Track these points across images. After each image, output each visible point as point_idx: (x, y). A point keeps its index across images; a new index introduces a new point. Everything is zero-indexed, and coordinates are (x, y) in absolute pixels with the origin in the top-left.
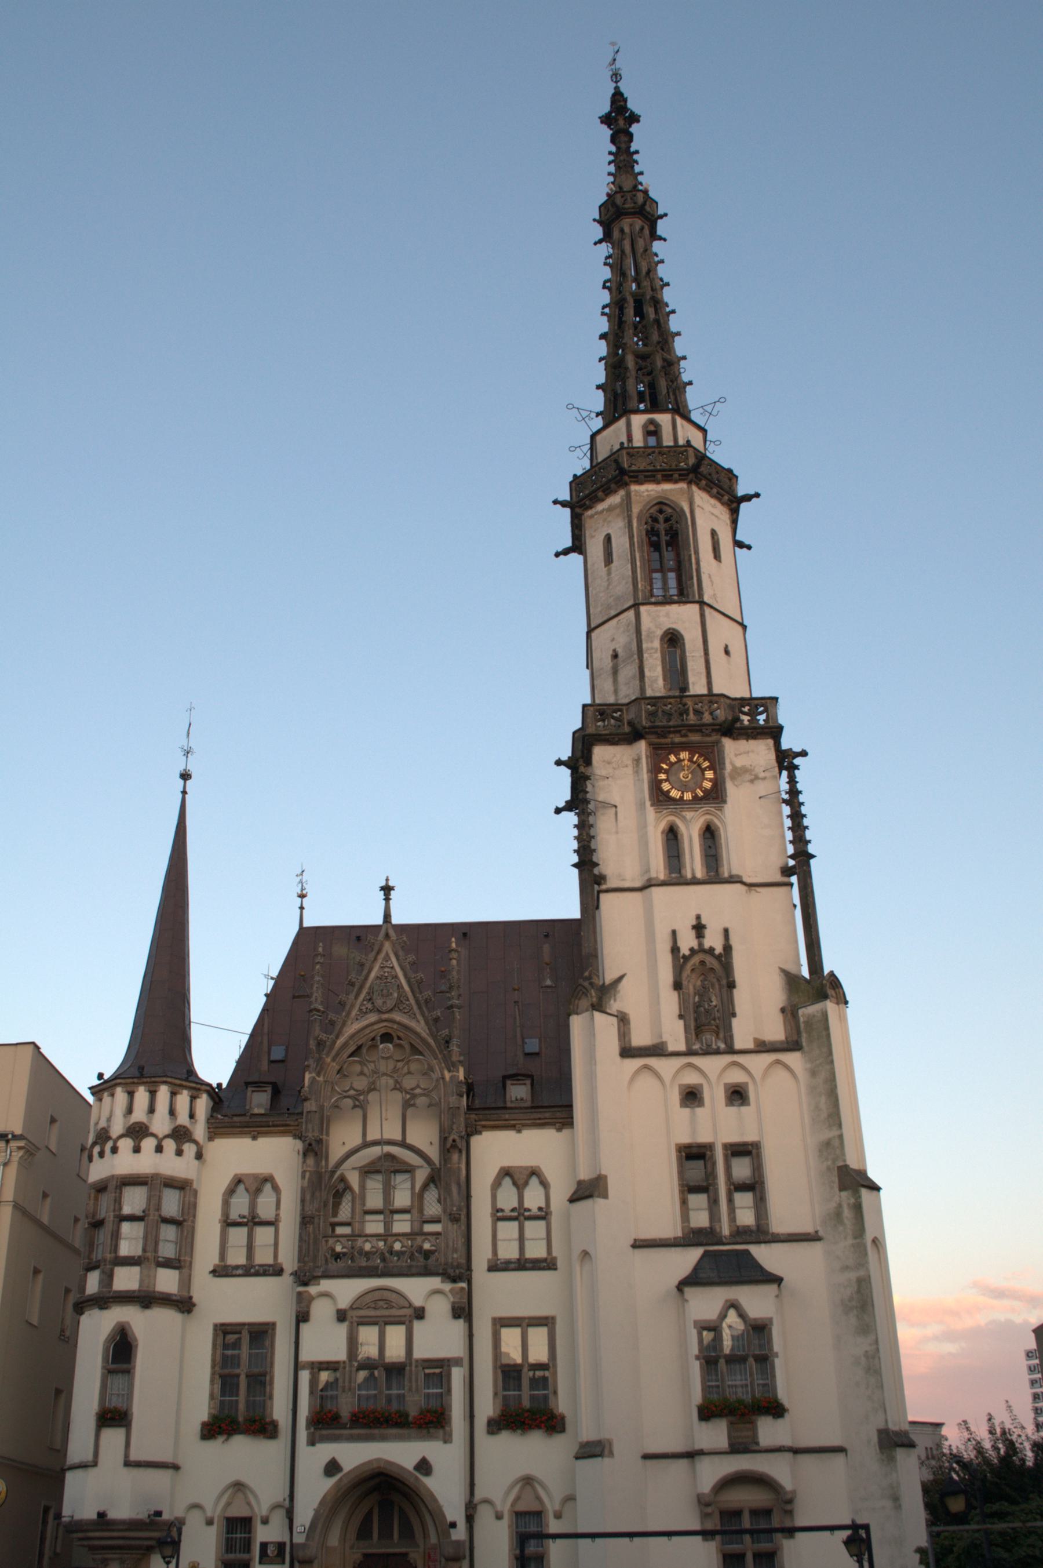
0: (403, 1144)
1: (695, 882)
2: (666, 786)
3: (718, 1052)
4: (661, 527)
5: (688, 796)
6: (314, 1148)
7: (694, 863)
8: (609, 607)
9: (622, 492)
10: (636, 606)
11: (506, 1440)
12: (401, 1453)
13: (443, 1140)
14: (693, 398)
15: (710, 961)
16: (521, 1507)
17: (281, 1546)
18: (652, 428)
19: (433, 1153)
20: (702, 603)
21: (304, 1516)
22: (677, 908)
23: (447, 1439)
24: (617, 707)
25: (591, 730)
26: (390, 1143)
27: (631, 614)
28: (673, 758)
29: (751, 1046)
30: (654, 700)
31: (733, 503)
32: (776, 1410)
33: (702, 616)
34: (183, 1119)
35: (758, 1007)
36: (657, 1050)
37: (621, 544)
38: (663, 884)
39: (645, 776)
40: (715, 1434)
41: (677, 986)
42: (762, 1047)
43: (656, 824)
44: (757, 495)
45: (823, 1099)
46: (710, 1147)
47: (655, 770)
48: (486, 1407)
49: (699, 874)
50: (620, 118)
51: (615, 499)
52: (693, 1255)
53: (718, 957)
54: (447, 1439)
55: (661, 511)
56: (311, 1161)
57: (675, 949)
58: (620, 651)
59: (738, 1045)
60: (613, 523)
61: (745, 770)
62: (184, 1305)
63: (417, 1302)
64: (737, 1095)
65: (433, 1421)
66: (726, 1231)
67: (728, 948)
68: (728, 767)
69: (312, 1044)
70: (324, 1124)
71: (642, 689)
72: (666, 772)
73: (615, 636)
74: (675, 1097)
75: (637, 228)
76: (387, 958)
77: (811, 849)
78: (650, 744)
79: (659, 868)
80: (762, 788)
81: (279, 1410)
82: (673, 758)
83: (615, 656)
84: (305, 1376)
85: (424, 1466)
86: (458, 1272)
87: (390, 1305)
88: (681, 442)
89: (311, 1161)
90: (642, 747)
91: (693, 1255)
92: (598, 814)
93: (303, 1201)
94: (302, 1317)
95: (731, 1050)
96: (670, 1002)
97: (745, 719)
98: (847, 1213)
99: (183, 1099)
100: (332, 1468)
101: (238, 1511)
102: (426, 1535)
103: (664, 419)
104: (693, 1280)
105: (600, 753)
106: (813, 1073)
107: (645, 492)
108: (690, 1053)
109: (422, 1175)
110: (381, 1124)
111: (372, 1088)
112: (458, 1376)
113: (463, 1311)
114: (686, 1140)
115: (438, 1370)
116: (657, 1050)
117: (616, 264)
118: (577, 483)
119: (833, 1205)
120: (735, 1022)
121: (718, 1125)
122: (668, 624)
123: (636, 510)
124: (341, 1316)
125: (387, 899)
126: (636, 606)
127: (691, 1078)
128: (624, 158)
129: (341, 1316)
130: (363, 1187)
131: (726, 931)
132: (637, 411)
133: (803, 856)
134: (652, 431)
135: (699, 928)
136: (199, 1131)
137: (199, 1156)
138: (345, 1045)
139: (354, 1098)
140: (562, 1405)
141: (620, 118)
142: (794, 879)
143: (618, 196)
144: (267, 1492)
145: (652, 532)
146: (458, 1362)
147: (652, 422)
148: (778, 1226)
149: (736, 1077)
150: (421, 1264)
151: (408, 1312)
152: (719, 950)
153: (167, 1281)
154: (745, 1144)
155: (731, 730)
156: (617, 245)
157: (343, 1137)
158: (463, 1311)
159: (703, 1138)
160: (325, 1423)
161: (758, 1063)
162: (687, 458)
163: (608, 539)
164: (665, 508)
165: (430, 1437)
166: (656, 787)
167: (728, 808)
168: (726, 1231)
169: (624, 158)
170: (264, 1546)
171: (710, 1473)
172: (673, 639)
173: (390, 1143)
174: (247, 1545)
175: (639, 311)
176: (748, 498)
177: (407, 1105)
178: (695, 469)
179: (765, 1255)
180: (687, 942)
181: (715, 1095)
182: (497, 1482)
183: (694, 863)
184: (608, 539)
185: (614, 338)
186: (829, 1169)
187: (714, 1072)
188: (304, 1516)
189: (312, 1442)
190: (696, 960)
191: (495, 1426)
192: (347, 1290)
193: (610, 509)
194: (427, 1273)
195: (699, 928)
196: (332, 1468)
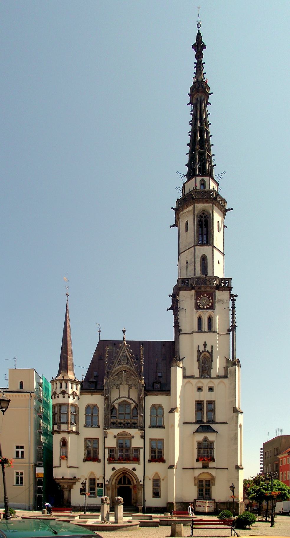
0: (129, 398)
1: (205, 332)
2: (199, 304)
3: (207, 378)
4: (203, 219)
5: (205, 307)
6: (107, 399)
7: (205, 327)
9: (192, 206)
10: (194, 246)
11: (153, 464)
12: (129, 466)
13: (139, 397)
14: (215, 171)
15: (207, 354)
16: (155, 478)
17: (102, 484)
18: (203, 182)
19: (136, 401)
20: (214, 247)
21: (107, 478)
22: (200, 339)
23: (139, 464)
24: (187, 280)
25: (180, 286)
26: (126, 397)
27: (193, 248)
28: (202, 296)
29: (215, 377)
30: (198, 278)
31: (224, 212)
32: (213, 460)
33: (213, 250)
34: (74, 390)
35: (218, 365)
36: (192, 377)
38: (197, 332)
39: (194, 301)
40: (200, 464)
41: (198, 360)
42: (218, 377)
43: (196, 315)
44: (232, 209)
46: (203, 401)
47: (197, 299)
48: (148, 457)
49: (206, 330)
50: (199, 46)
51: (190, 208)
52: (197, 426)
53: (209, 353)
54: (139, 464)
55: (203, 214)
56: (106, 401)
57: (198, 351)
59: (212, 377)
60: (189, 217)
61: (221, 300)
62: (77, 433)
63: (132, 435)
64: (211, 389)
65: (137, 459)
66: (205, 421)
67: (212, 351)
68: (217, 299)
69: (106, 372)
70: (109, 392)
71: (195, 275)
72: (200, 300)
73: (188, 256)
74: (196, 389)
75: (203, 98)
76: (124, 350)
78: (196, 291)
79: (196, 328)
80: (225, 306)
81: (101, 456)
82: (202, 296)
84: (107, 450)
85: (134, 469)
86: (143, 428)
87: (126, 435)
88: (211, 188)
89: (106, 401)
90: (193, 292)
91: (197, 426)
92: (181, 312)
93: (104, 411)
94: (105, 437)
95: (210, 378)
96: (196, 365)
97: (223, 284)
98: (234, 418)
99: (74, 386)
100: (114, 469)
101: (92, 477)
102: (133, 483)
103: (206, 179)
104: (197, 431)
105: (182, 293)
106: (230, 384)
107: (200, 206)
108: (200, 378)
109: (133, 406)
110: (123, 393)
111: (121, 384)
112: (142, 451)
113: (143, 437)
114: (198, 399)
115: (137, 450)
116: (192, 377)
117: (194, 114)
118: (179, 202)
120: (212, 370)
121: (205, 396)
122: (203, 253)
123: (196, 215)
124: (115, 437)
125: (124, 334)
126: (194, 246)
127: (200, 385)
128: (199, 66)
129: (115, 437)
130: (119, 408)
131: (212, 346)
132: (198, 176)
133: (234, 327)
134: (203, 184)
135: (205, 345)
136: (78, 393)
137: (79, 399)
138: (114, 373)
139: (117, 386)
140: (165, 457)
141: (199, 46)
142: (231, 333)
143: (197, 83)
144: (98, 474)
145: (200, 221)
146: (141, 448)
147: (203, 180)
148: (217, 420)
149: (211, 385)
150: (134, 426)
151: (130, 437)
152: (210, 351)
153: (74, 429)
154: (212, 401)
155: (218, 287)
156: (195, 106)
157: (114, 395)
158: (143, 437)
159: (202, 399)
160: (112, 460)
161: (217, 381)
162: (213, 194)
164: (205, 212)
165: (136, 463)
166: (196, 304)
167: (215, 311)
168: (205, 421)
169: (199, 66)
170: (98, 484)
171: (197, 473)
172: (204, 259)
173: (126, 397)
174: (94, 484)
175: (201, 135)
176: (229, 210)
177: (129, 388)
178: (215, 199)
179: (213, 426)
180: (202, 349)
181: (205, 389)
182: (150, 474)
183: (205, 327)
185: (192, 145)
187: (205, 383)
188: (107, 478)
189: (109, 464)
190: (203, 354)
191: (150, 461)
192: (116, 431)
193: (188, 212)
194: (134, 428)
195: (205, 345)
196: (114, 469)
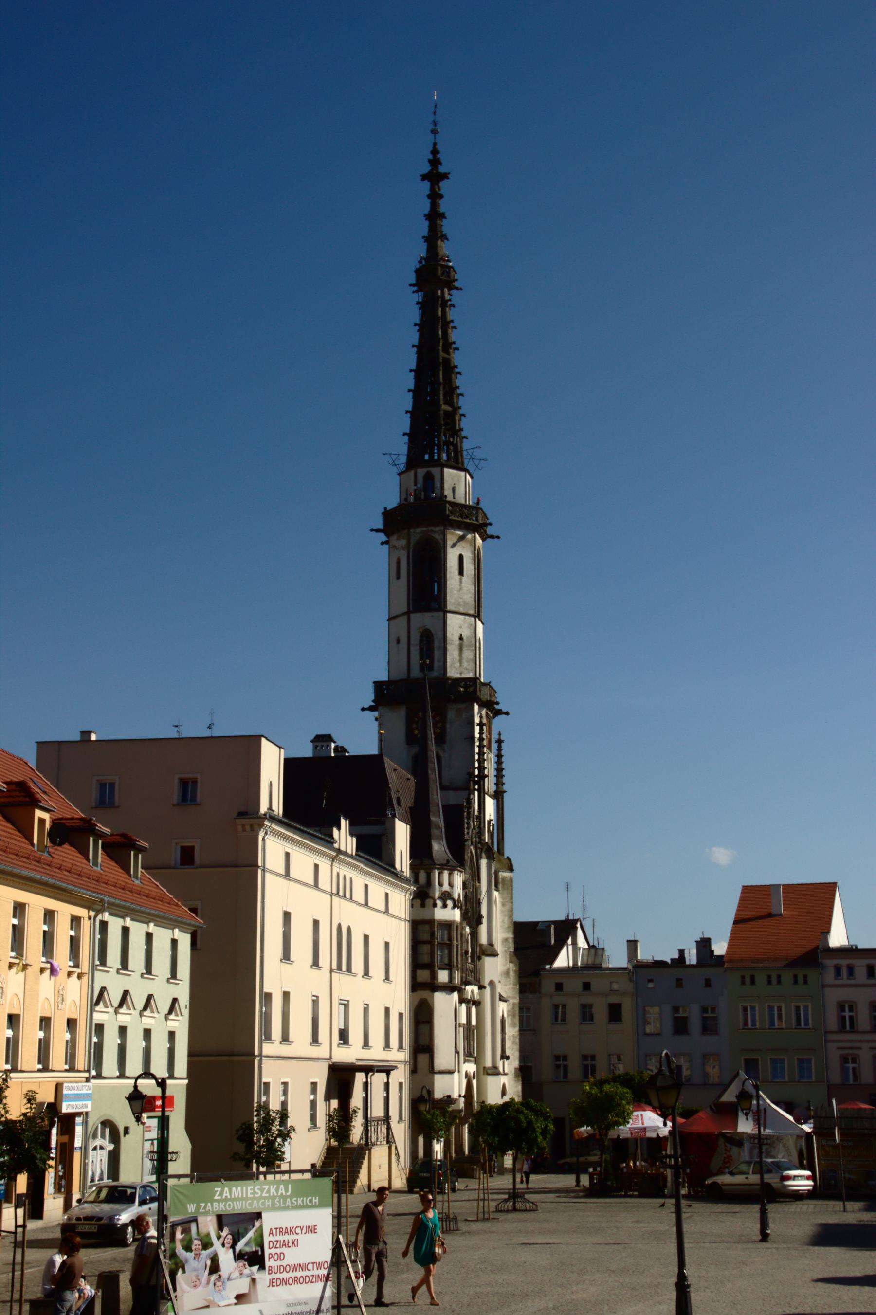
8: (459, 604)
37: (469, 567)
45: (506, 919)
58: (464, 638)
77: (505, 788)
83: (461, 638)
119: (506, 968)
141: (435, 176)
163: (461, 557)
184: (461, 557)
186: (506, 951)
